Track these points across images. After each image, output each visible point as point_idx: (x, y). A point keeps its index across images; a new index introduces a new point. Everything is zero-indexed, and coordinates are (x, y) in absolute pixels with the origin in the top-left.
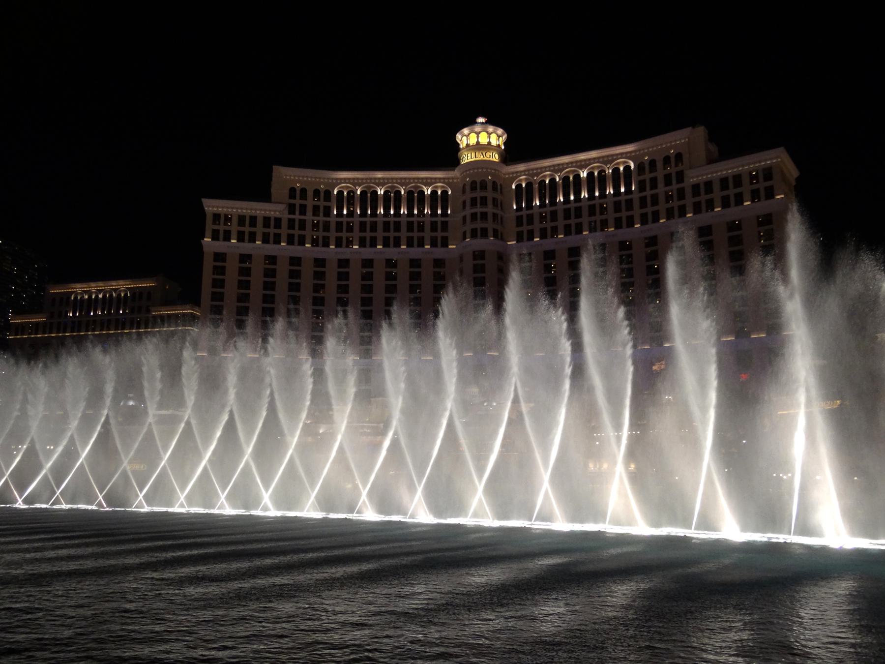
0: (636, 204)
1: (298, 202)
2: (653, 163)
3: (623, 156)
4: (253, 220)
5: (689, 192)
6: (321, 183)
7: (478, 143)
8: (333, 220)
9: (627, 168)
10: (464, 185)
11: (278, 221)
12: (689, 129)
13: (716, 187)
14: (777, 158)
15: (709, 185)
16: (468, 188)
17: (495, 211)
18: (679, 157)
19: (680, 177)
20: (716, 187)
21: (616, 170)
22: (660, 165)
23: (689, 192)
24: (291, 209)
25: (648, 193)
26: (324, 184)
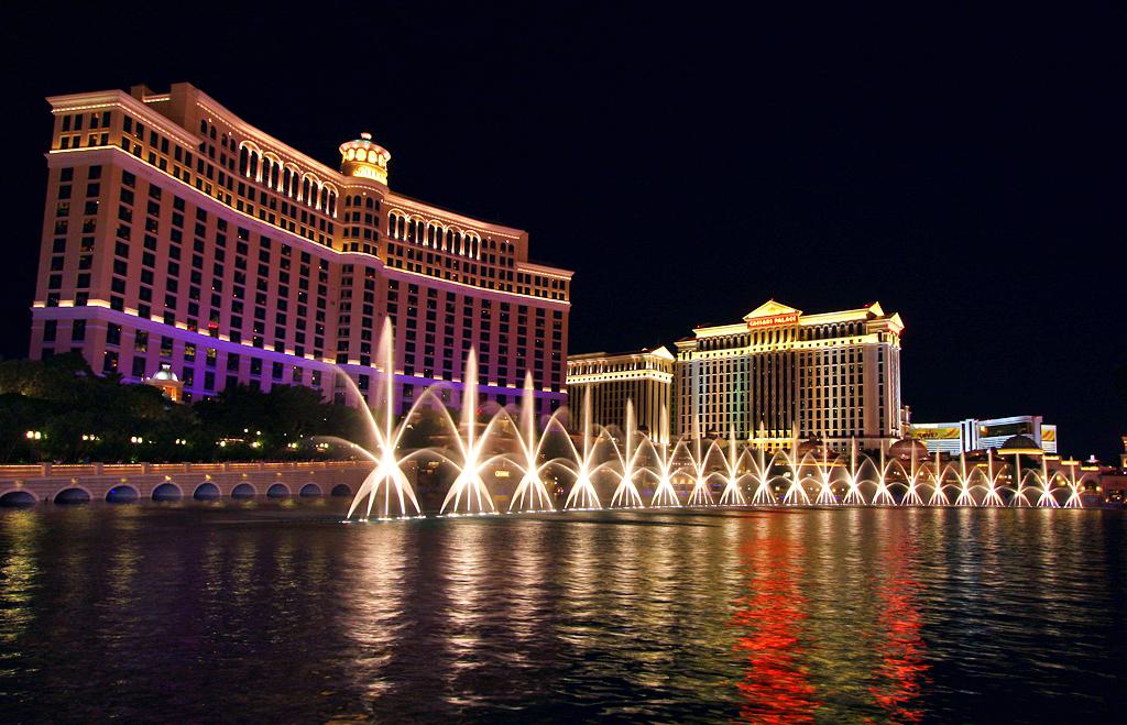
0: (479, 271)
1: (210, 142)
2: (493, 243)
3: (473, 228)
4: (166, 142)
5: (515, 277)
6: (231, 130)
7: (377, 164)
8: (237, 178)
9: (475, 239)
10: (358, 200)
11: (189, 155)
12: (523, 232)
13: (533, 281)
14: (567, 276)
15: (528, 276)
16: (364, 202)
17: (367, 227)
18: (511, 248)
19: (511, 263)
20: (533, 281)
21: (468, 237)
22: (498, 247)
23: (515, 277)
24: (202, 148)
25: (488, 266)
26: (233, 132)
